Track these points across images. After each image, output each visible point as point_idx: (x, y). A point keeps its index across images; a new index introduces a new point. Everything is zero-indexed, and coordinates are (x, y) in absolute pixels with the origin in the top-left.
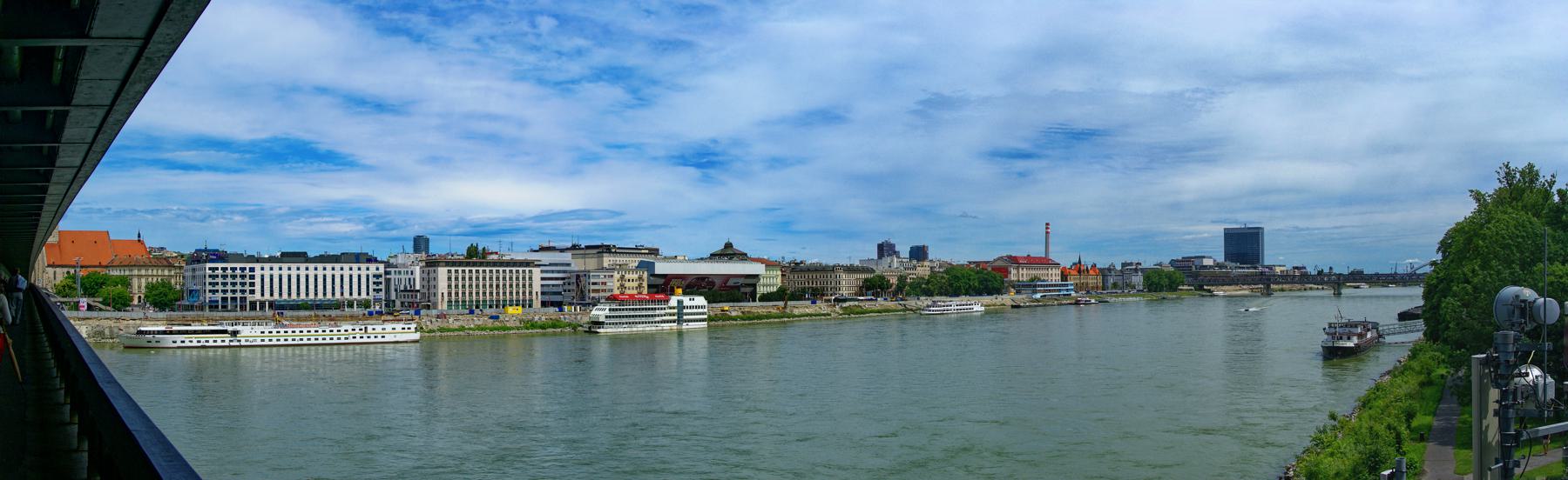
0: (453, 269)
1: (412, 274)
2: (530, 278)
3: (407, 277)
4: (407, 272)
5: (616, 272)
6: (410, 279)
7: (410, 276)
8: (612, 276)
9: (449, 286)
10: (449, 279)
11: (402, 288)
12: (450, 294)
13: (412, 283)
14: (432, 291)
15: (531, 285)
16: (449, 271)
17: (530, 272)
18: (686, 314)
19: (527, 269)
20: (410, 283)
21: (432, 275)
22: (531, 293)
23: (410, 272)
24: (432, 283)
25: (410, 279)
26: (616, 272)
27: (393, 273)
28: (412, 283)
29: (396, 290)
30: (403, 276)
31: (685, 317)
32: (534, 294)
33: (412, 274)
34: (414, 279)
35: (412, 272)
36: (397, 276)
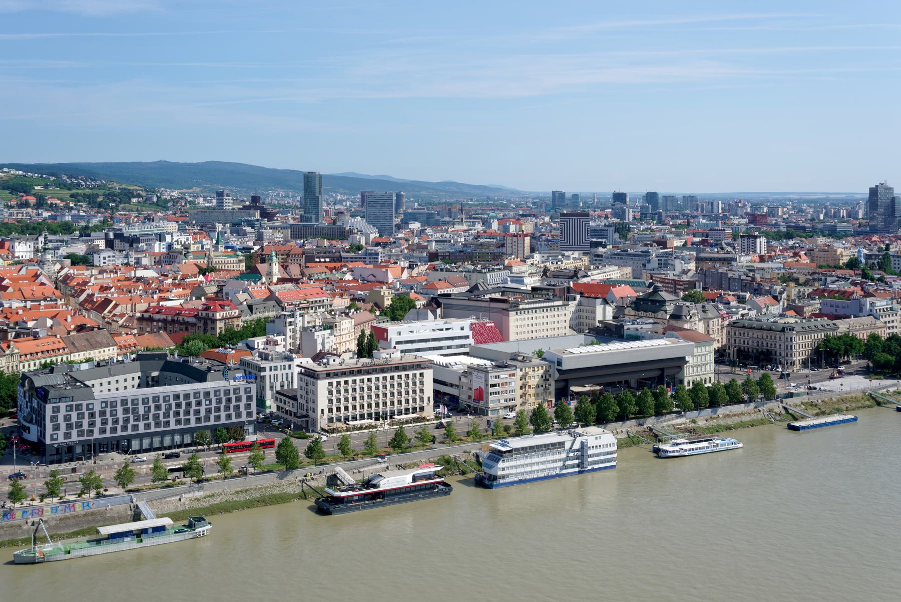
0: (334, 381)
1: (290, 368)
2: (422, 383)
3: (284, 372)
4: (285, 366)
5: (518, 370)
6: (287, 374)
7: (287, 371)
8: (514, 375)
9: (331, 401)
10: (331, 392)
11: (279, 388)
12: (331, 410)
13: (290, 379)
14: (310, 404)
15: (422, 391)
16: (331, 384)
17: (422, 375)
18: (590, 456)
19: (418, 372)
20: (287, 378)
21: (310, 387)
22: (422, 400)
23: (287, 367)
24: (310, 396)
25: (287, 374)
26: (518, 370)
27: (268, 369)
28: (290, 379)
29: (271, 387)
30: (279, 372)
31: (590, 459)
32: (426, 400)
33: (290, 368)
34: (292, 373)
35: (290, 366)
36: (273, 373)
